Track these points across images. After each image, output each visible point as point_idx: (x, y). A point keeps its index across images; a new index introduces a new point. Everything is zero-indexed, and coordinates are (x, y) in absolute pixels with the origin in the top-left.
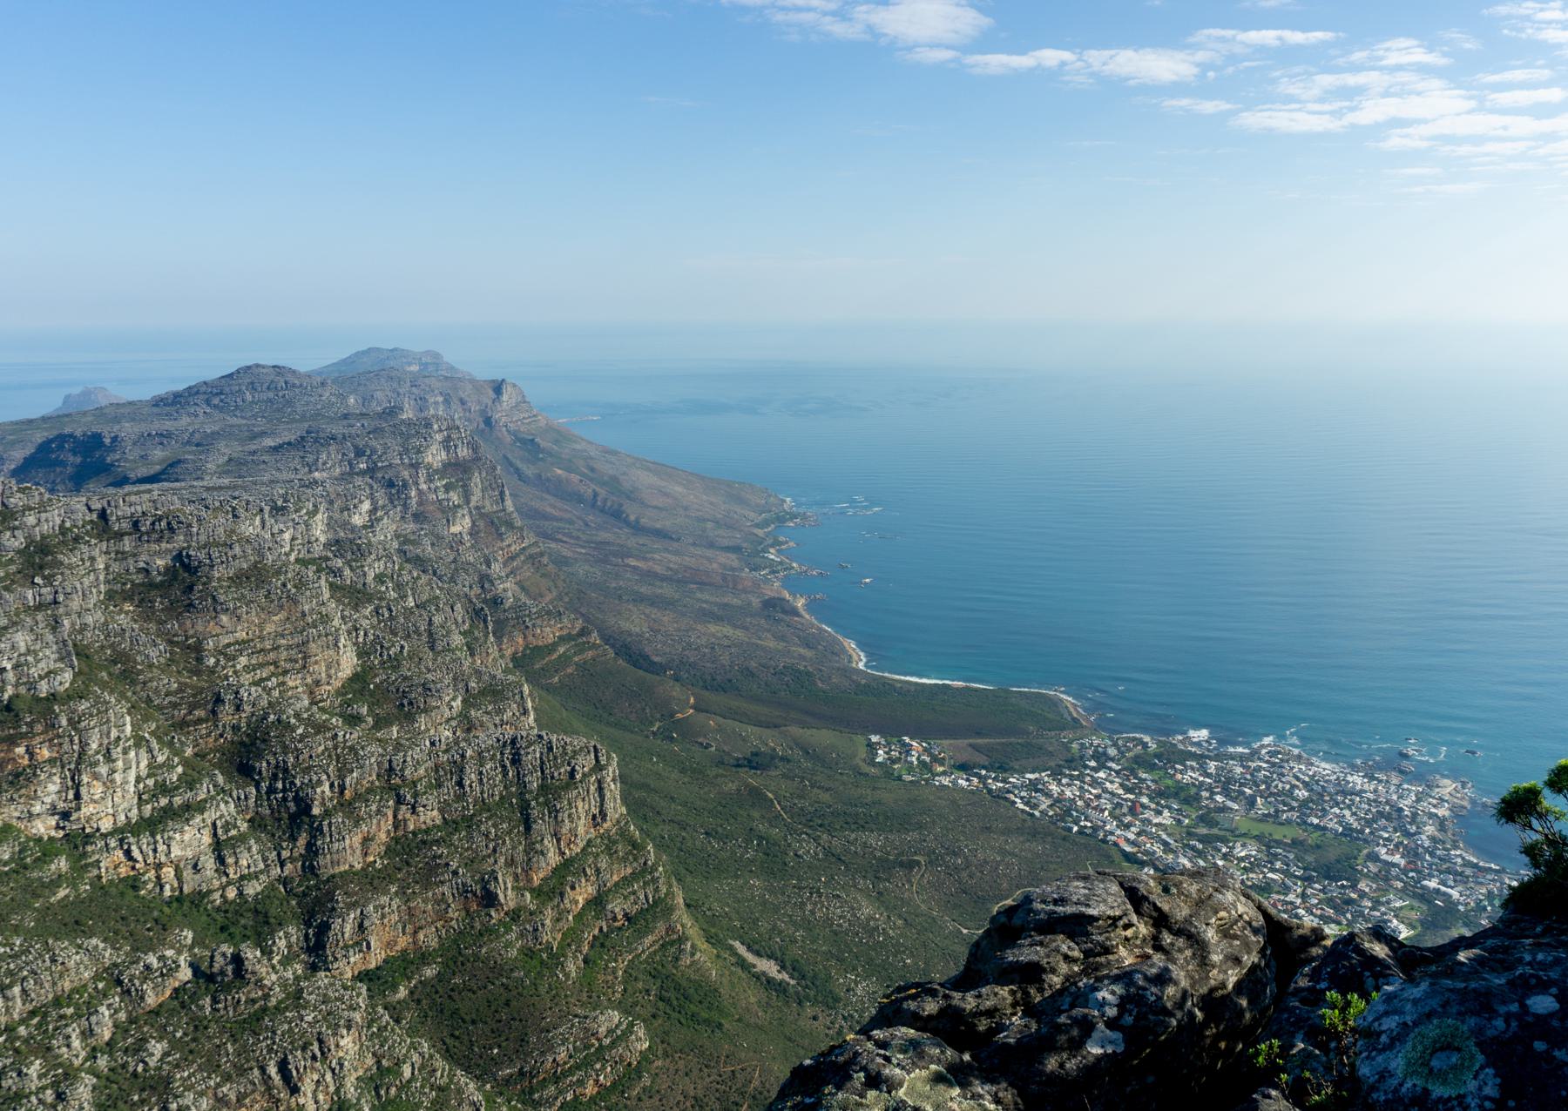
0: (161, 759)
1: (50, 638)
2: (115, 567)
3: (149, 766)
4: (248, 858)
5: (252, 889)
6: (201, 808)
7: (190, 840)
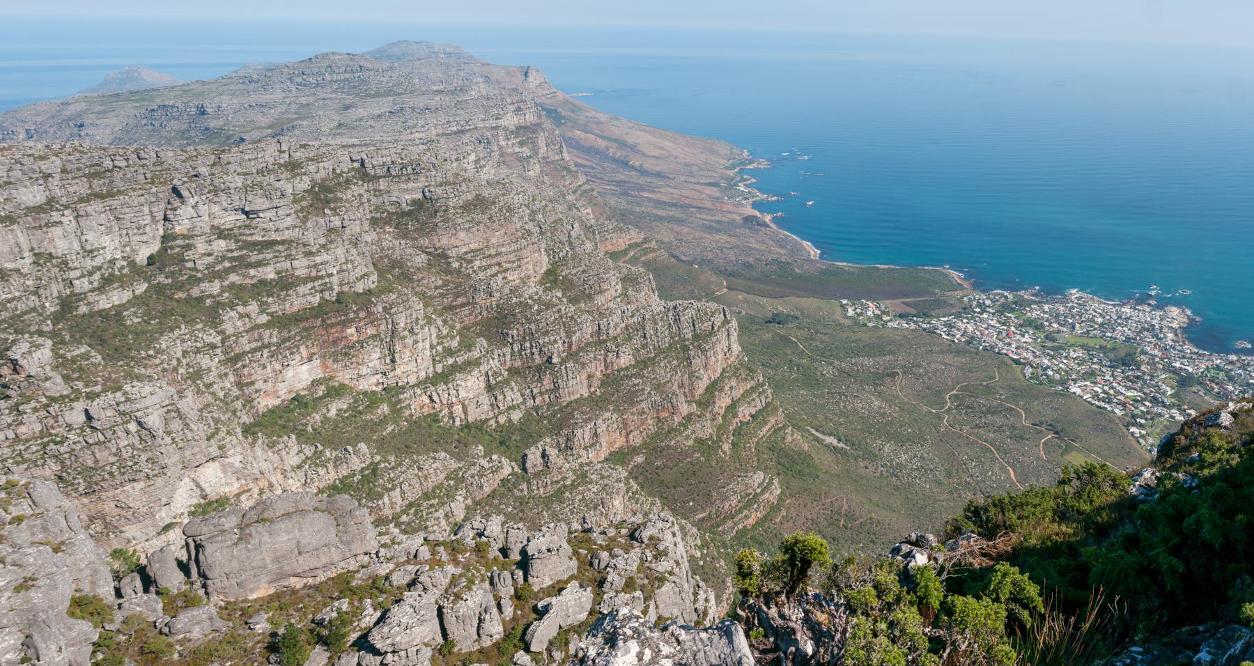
0: (445, 331)
1: (354, 251)
2: (374, 200)
3: (438, 337)
4: (513, 395)
5: (516, 416)
6: (477, 363)
7: (471, 386)
